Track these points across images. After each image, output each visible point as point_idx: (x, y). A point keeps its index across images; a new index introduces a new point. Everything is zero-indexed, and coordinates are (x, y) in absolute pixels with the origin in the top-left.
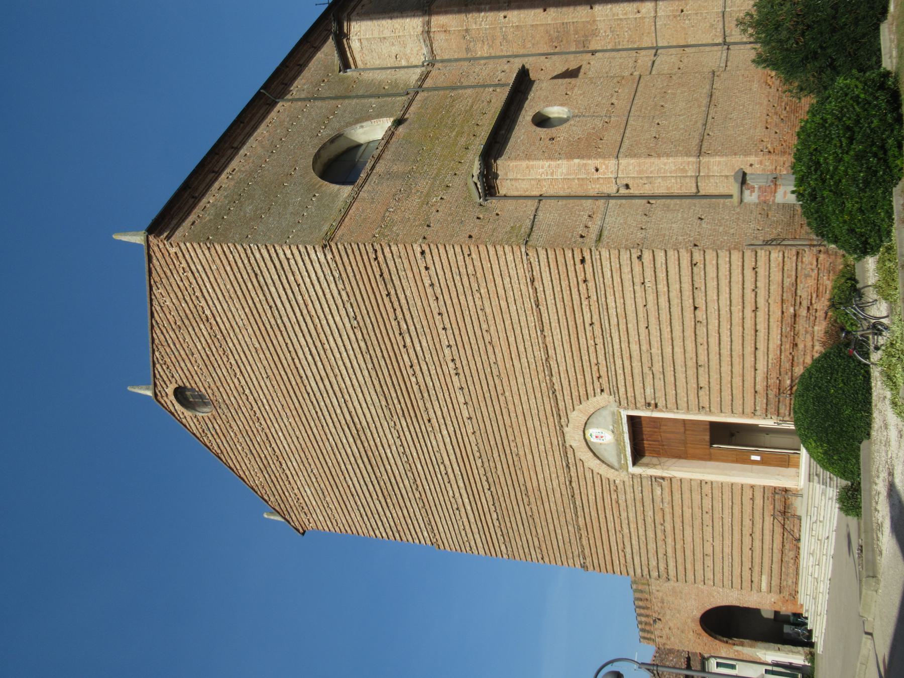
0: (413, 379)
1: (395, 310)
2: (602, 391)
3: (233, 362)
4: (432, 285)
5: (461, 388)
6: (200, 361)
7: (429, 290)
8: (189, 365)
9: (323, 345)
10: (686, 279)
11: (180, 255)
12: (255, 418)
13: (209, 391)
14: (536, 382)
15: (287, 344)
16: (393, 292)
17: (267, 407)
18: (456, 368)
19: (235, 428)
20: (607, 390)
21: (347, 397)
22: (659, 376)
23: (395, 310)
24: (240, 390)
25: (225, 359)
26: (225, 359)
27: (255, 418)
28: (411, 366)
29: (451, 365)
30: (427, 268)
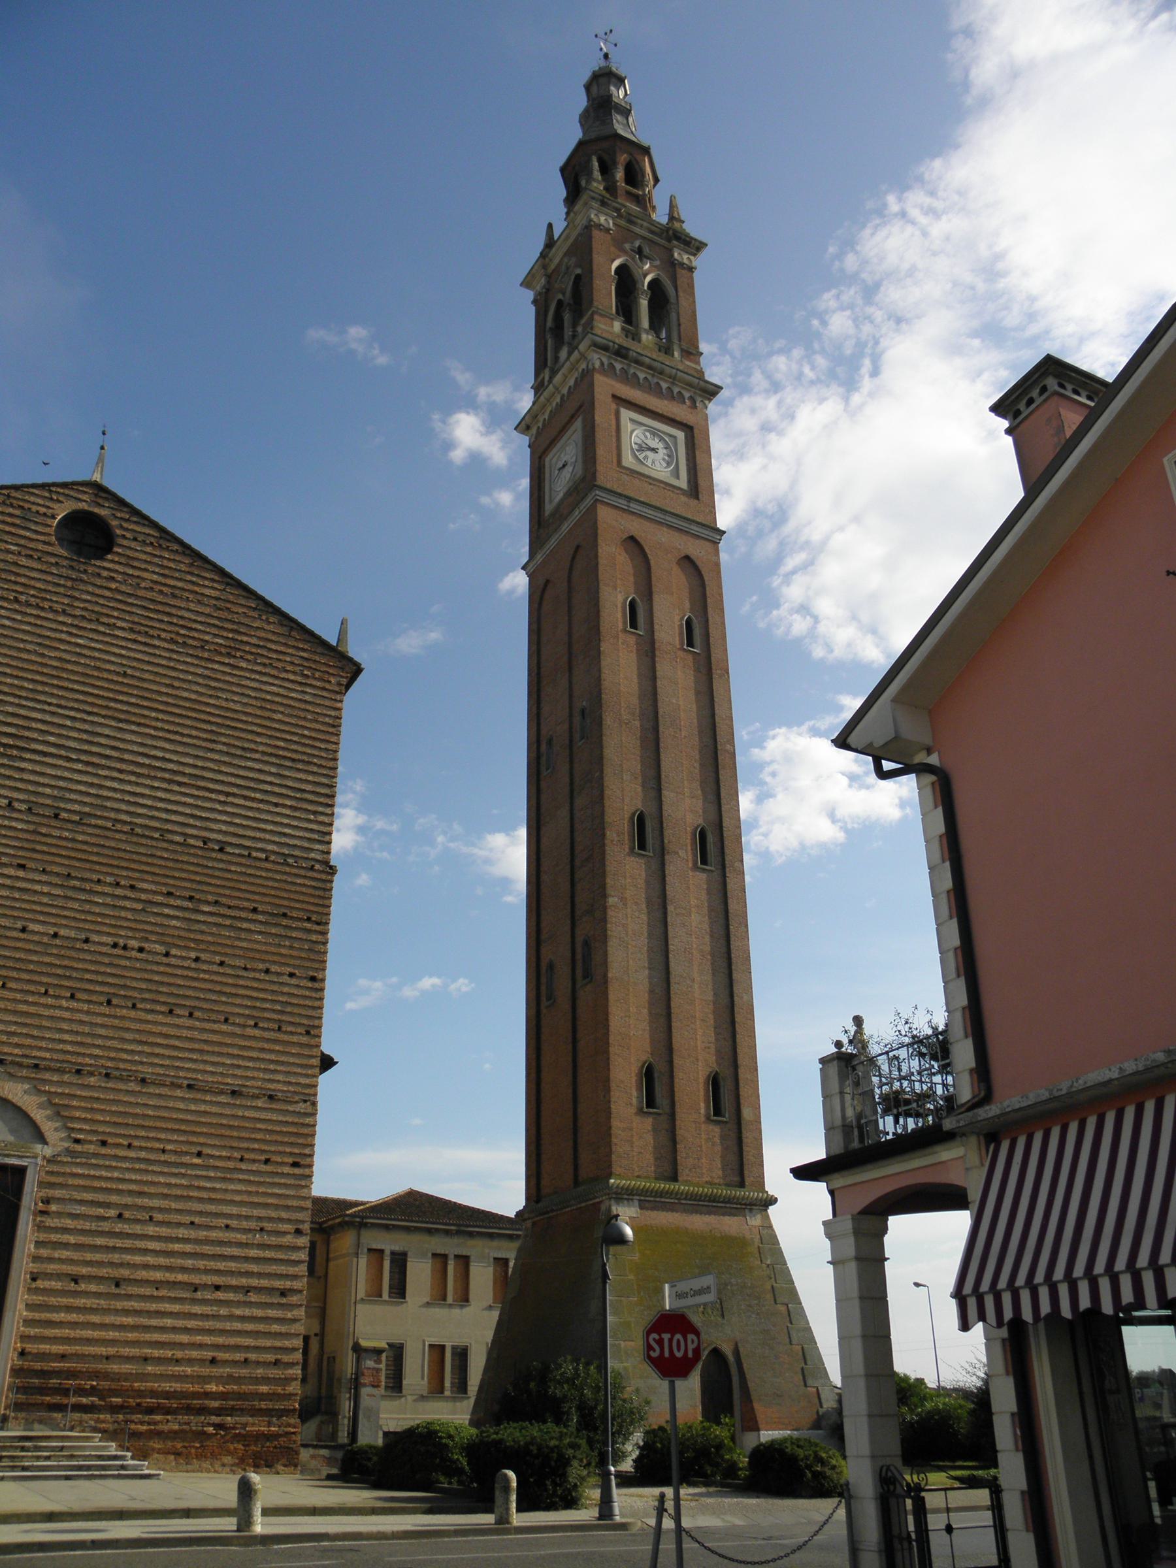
0: (109, 879)
1: (229, 907)
2: (77, 1141)
3: (156, 642)
4: (267, 971)
5: (87, 941)
6: (160, 598)
7: (261, 966)
8: (155, 577)
9: (180, 784)
10: (264, 1283)
11: (327, 686)
12: (46, 605)
13: (105, 574)
14: (97, 1052)
15: (182, 735)
16: (255, 917)
17: (64, 636)
18: (125, 948)
19: (24, 561)
20: (79, 1148)
21: (80, 766)
22: (105, 1226)
23: (229, 907)
24: (105, 620)
25: (163, 635)
26: (163, 635)
27: (46, 605)
28: (132, 887)
29: (134, 944)
30: (291, 975)
